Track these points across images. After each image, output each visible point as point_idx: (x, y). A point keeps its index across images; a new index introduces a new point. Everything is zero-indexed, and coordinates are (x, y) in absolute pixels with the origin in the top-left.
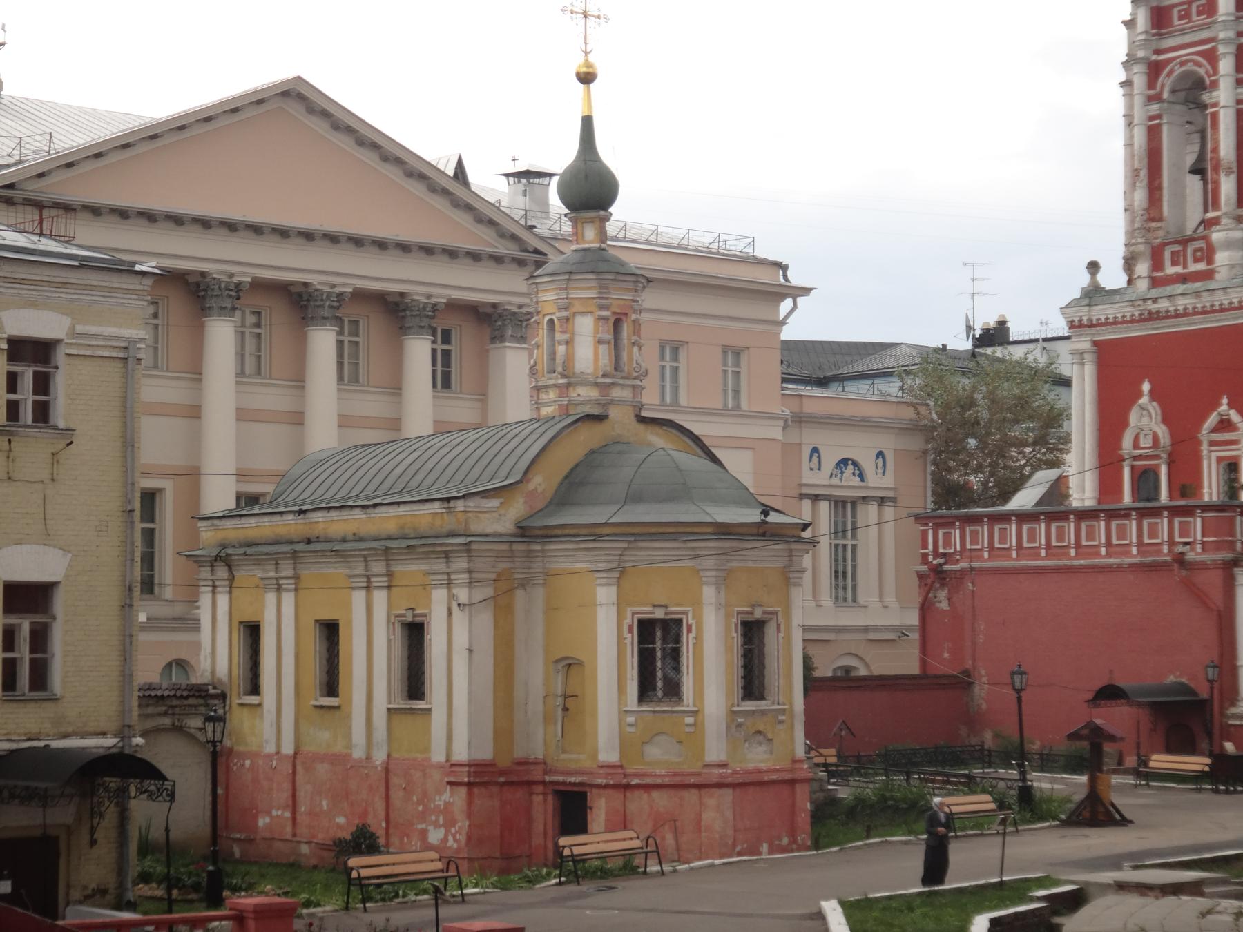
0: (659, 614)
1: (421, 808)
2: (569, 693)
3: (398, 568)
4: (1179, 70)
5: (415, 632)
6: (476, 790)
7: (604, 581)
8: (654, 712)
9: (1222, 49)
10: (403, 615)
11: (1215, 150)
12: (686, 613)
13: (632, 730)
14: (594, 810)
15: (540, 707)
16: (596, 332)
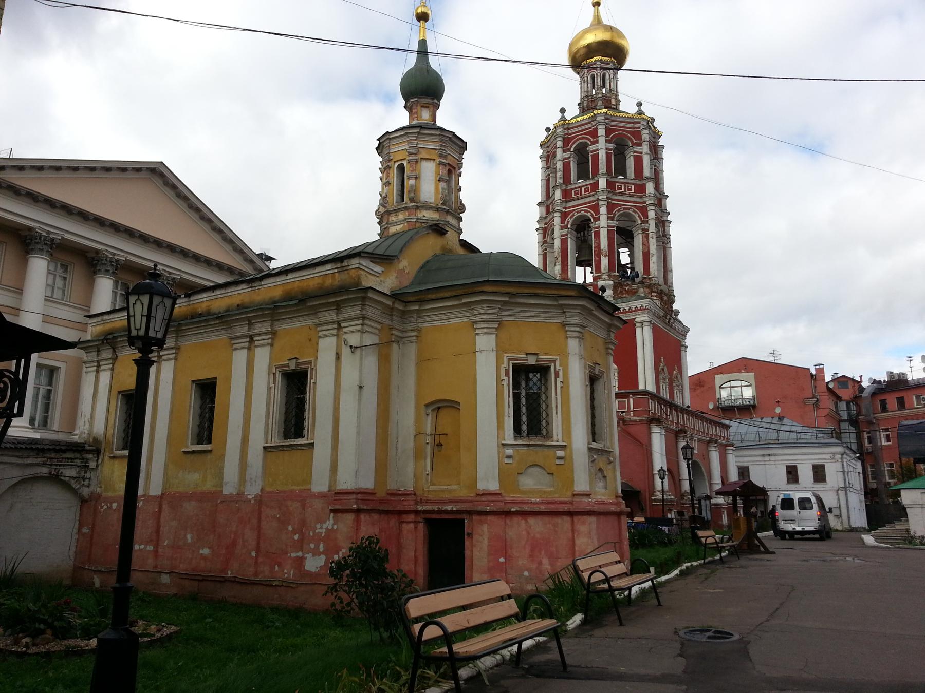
0: (532, 361)
1: (296, 537)
2: (439, 431)
3: (281, 327)
4: (576, 215)
5: (296, 382)
6: (362, 517)
7: (485, 331)
8: (529, 445)
9: (601, 203)
10: (288, 365)
11: (598, 246)
12: (554, 361)
13: (510, 461)
14: (475, 537)
15: (411, 444)
16: (437, 173)
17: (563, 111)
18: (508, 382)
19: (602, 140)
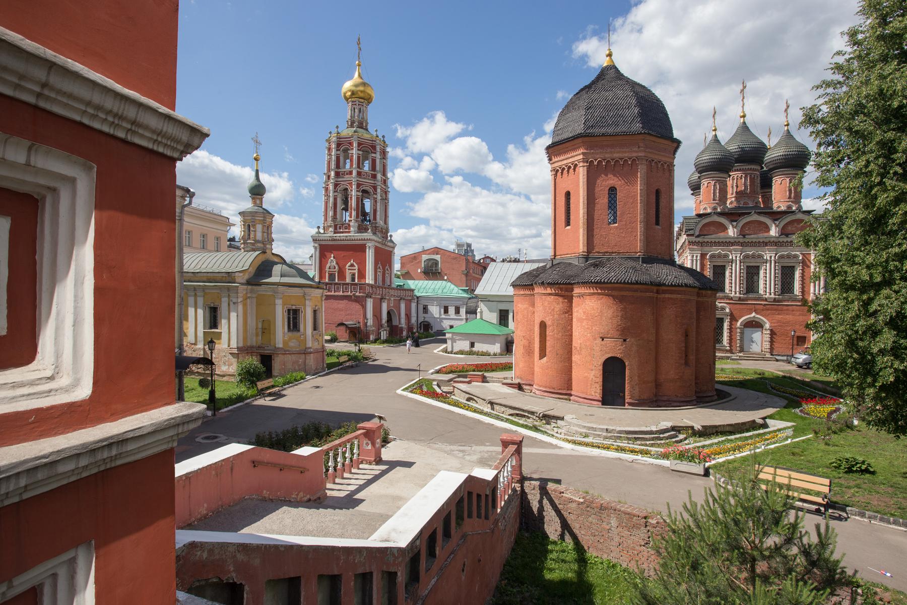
17: (337, 127)
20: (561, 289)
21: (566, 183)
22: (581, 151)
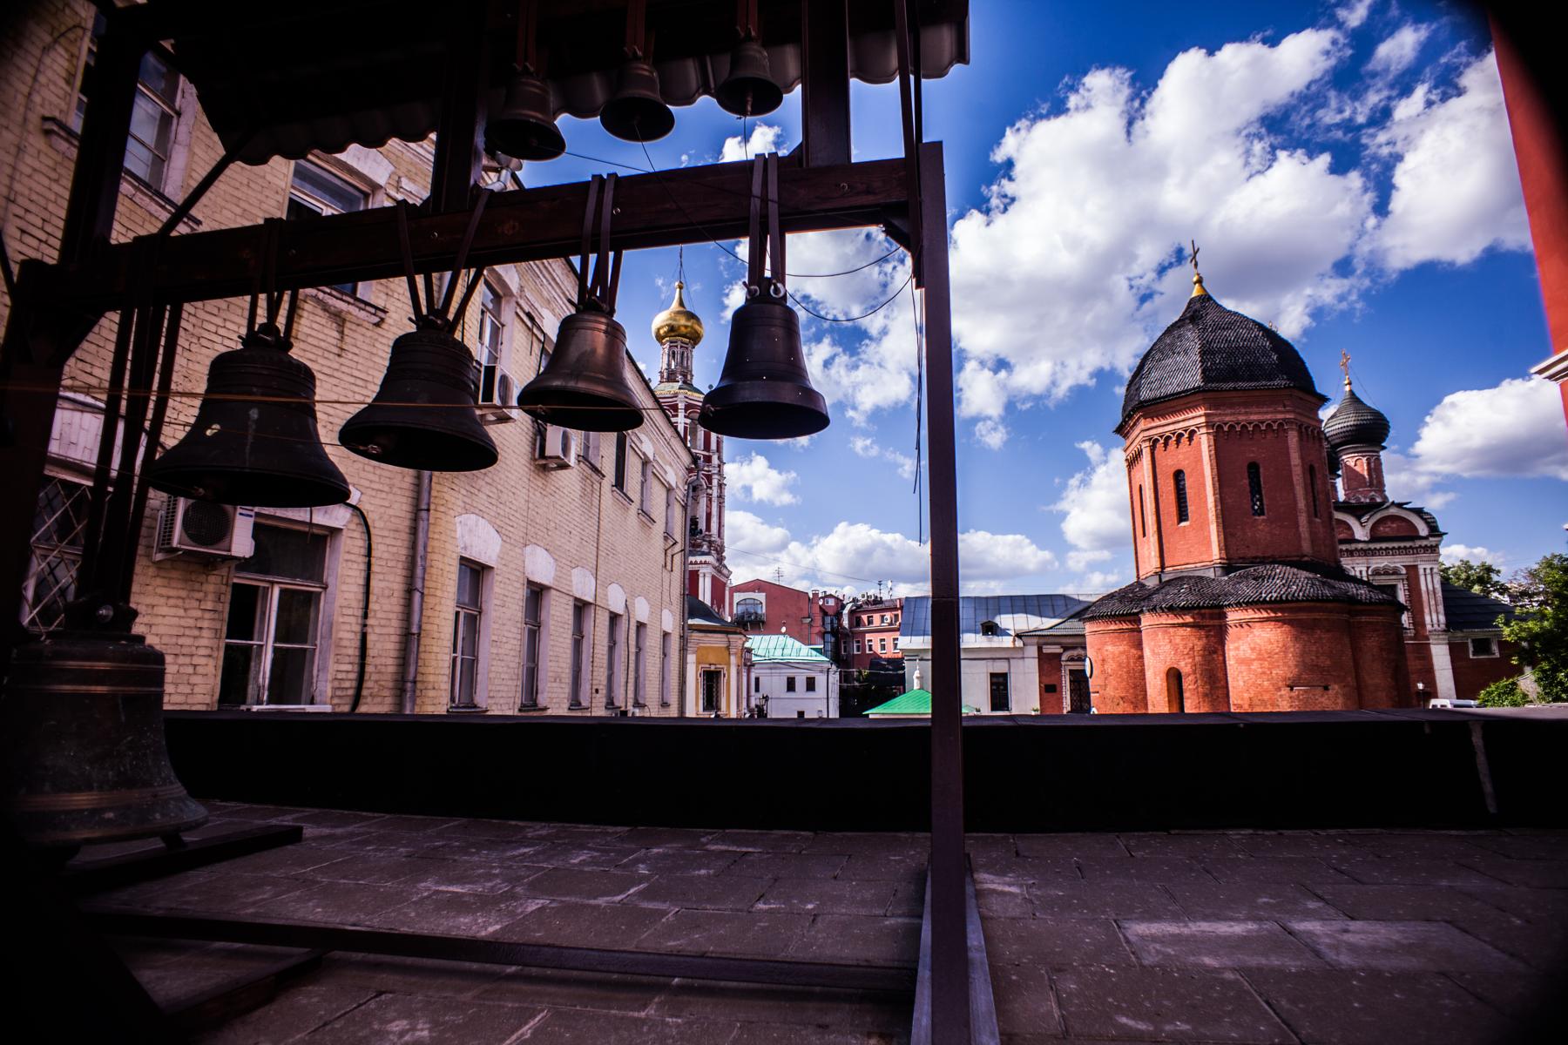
18: (701, 680)
19: (681, 414)
20: (1203, 616)
21: (1172, 459)
22: (1202, 412)
